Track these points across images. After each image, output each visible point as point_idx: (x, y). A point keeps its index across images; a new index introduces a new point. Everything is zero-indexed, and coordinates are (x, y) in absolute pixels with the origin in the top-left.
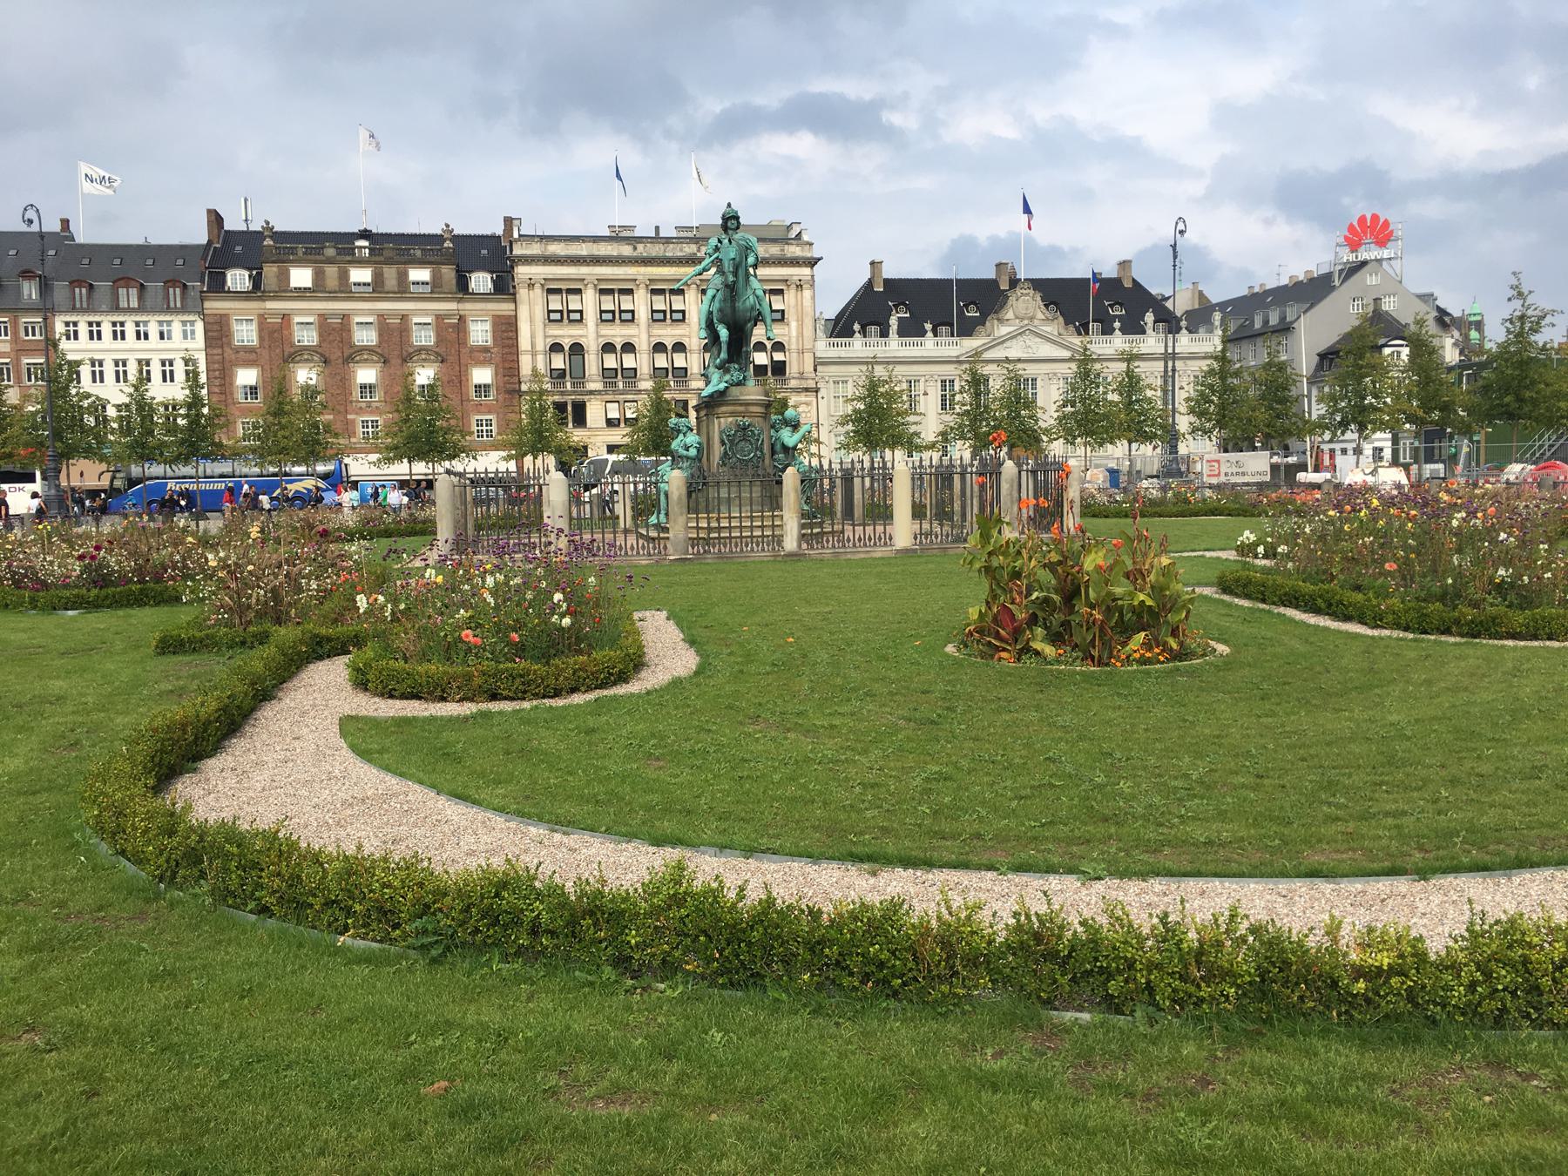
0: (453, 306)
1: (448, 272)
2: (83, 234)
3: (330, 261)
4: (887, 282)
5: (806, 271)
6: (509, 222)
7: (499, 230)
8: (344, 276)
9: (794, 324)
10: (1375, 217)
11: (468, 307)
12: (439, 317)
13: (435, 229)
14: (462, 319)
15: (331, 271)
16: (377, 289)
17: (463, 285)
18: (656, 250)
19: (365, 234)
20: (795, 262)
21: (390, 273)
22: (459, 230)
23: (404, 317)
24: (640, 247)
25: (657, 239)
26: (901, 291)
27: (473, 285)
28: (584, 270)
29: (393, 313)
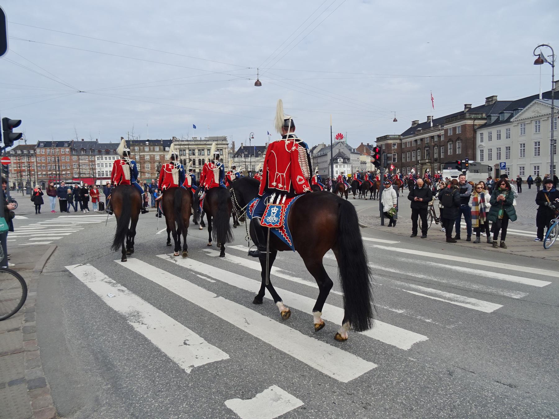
0: (162, 153)
1: (162, 147)
2: (100, 142)
3: (141, 146)
4: (244, 147)
5: (227, 146)
6: (173, 137)
7: (96, 140)
8: (144, 149)
9: (224, 156)
10: (340, 134)
11: (165, 153)
12: (160, 155)
13: (161, 139)
14: (164, 155)
15: (142, 147)
16: (150, 151)
17: (164, 150)
18: (202, 143)
19: (148, 141)
20: (224, 144)
21: (152, 148)
22: (163, 139)
23: (154, 155)
24: (196, 142)
25: (201, 141)
26: (246, 148)
27: (166, 149)
28: (186, 146)
29: (152, 155)
